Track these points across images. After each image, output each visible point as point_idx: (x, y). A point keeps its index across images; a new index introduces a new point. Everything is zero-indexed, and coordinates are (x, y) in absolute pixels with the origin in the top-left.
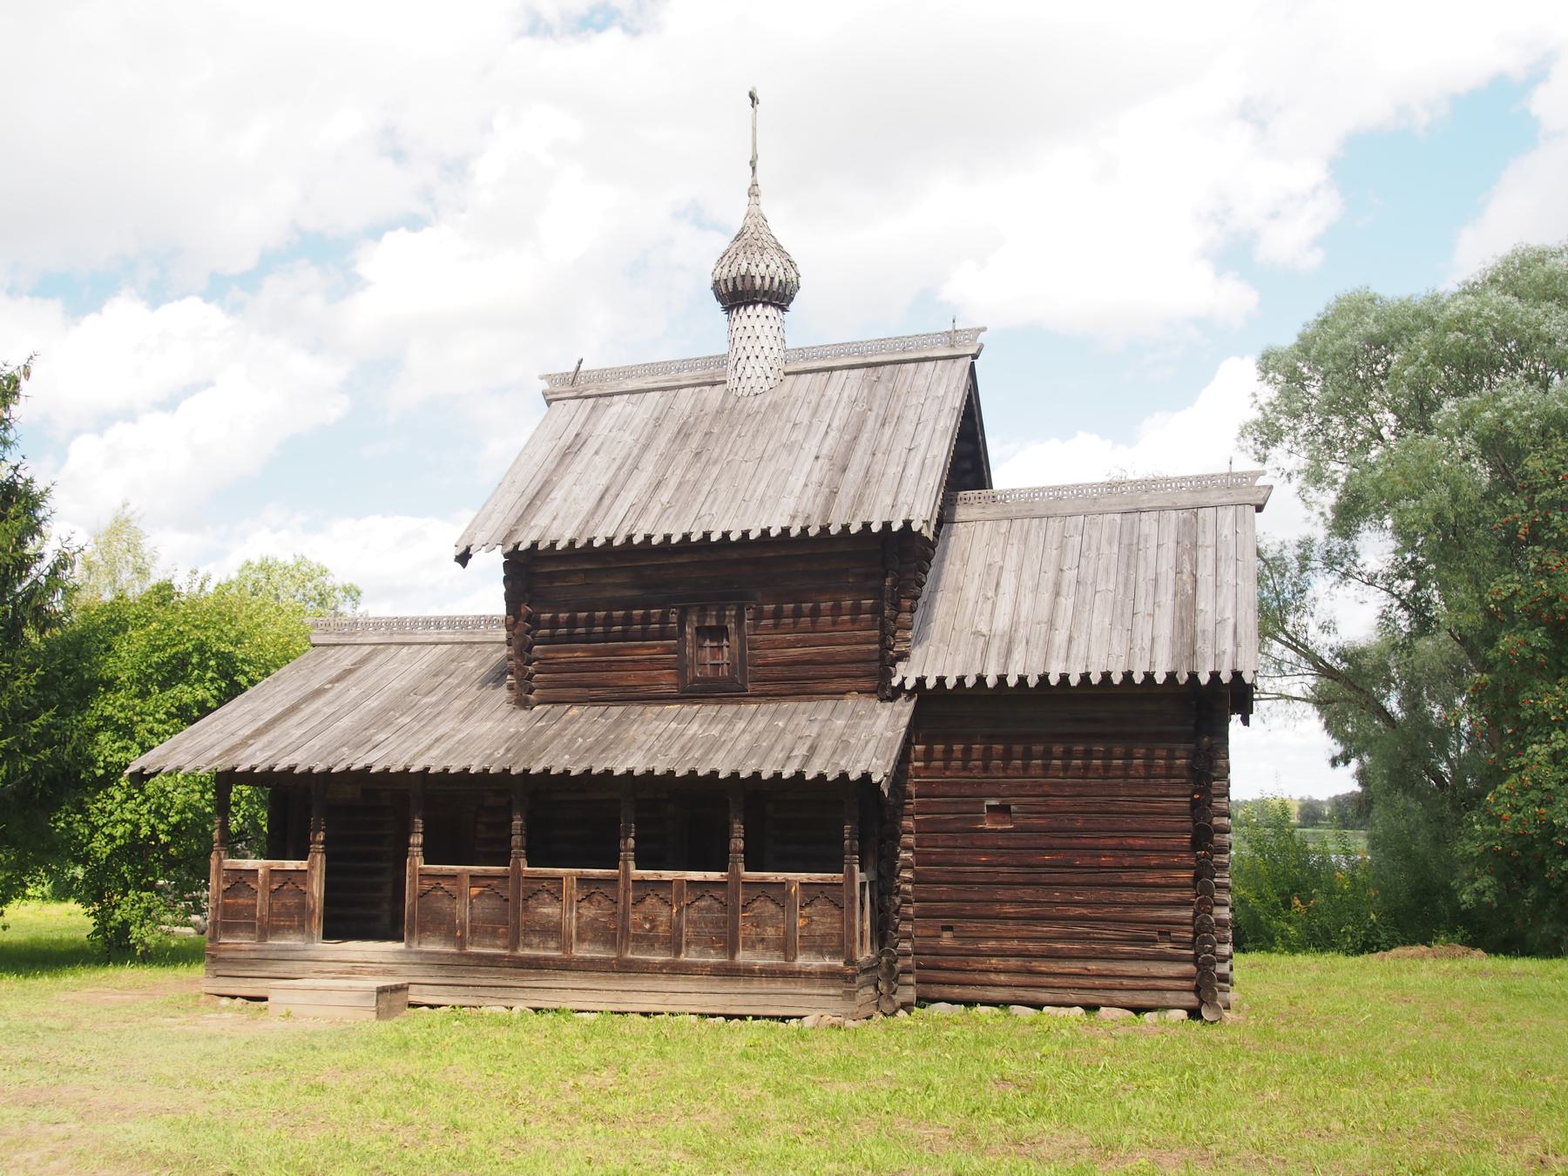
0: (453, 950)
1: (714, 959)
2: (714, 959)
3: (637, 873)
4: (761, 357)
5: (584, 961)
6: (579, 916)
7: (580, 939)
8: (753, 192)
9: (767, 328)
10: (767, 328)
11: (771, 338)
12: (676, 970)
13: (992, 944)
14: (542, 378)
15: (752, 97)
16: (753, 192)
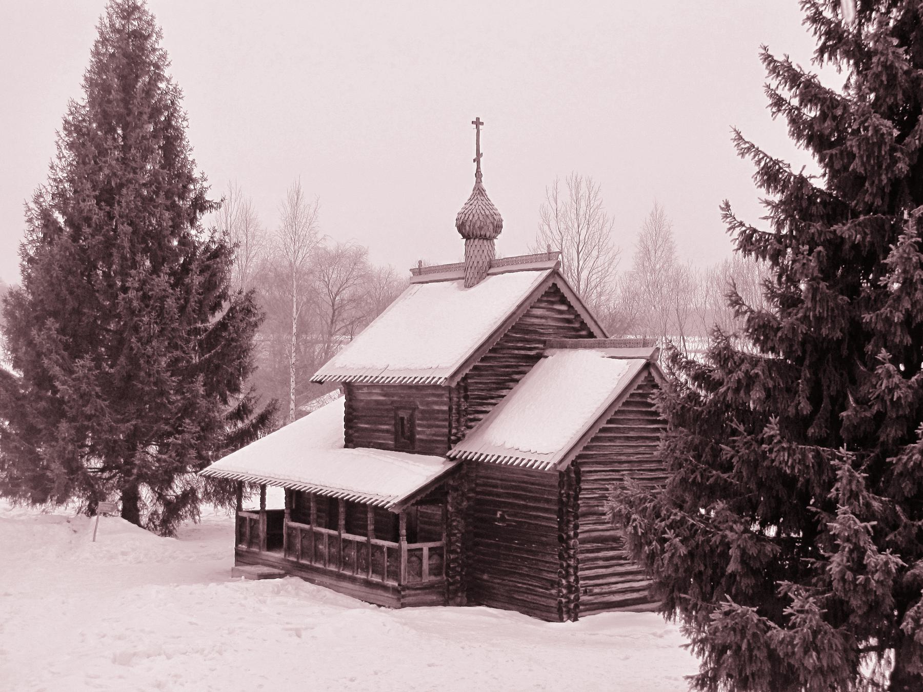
0: (295, 560)
1: (363, 576)
2: (363, 576)
3: (345, 536)
4: (473, 268)
5: (331, 571)
6: (329, 552)
7: (330, 561)
8: (478, 174)
9: (476, 252)
10: (476, 252)
11: (478, 257)
12: (353, 580)
13: (499, 581)
14: (411, 270)
15: (478, 123)
16: (478, 174)
